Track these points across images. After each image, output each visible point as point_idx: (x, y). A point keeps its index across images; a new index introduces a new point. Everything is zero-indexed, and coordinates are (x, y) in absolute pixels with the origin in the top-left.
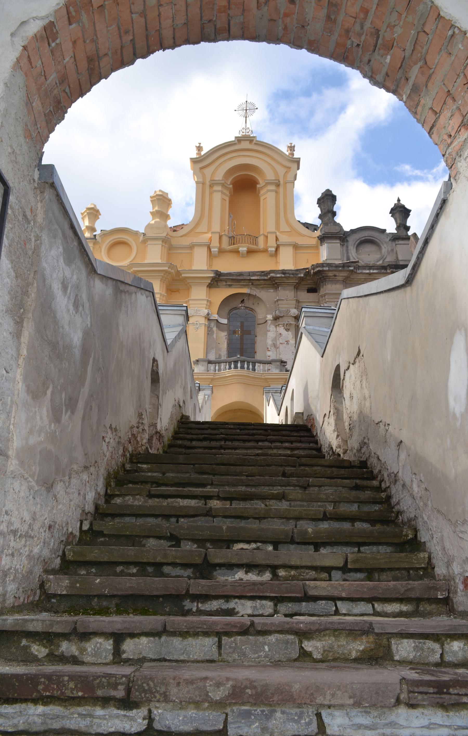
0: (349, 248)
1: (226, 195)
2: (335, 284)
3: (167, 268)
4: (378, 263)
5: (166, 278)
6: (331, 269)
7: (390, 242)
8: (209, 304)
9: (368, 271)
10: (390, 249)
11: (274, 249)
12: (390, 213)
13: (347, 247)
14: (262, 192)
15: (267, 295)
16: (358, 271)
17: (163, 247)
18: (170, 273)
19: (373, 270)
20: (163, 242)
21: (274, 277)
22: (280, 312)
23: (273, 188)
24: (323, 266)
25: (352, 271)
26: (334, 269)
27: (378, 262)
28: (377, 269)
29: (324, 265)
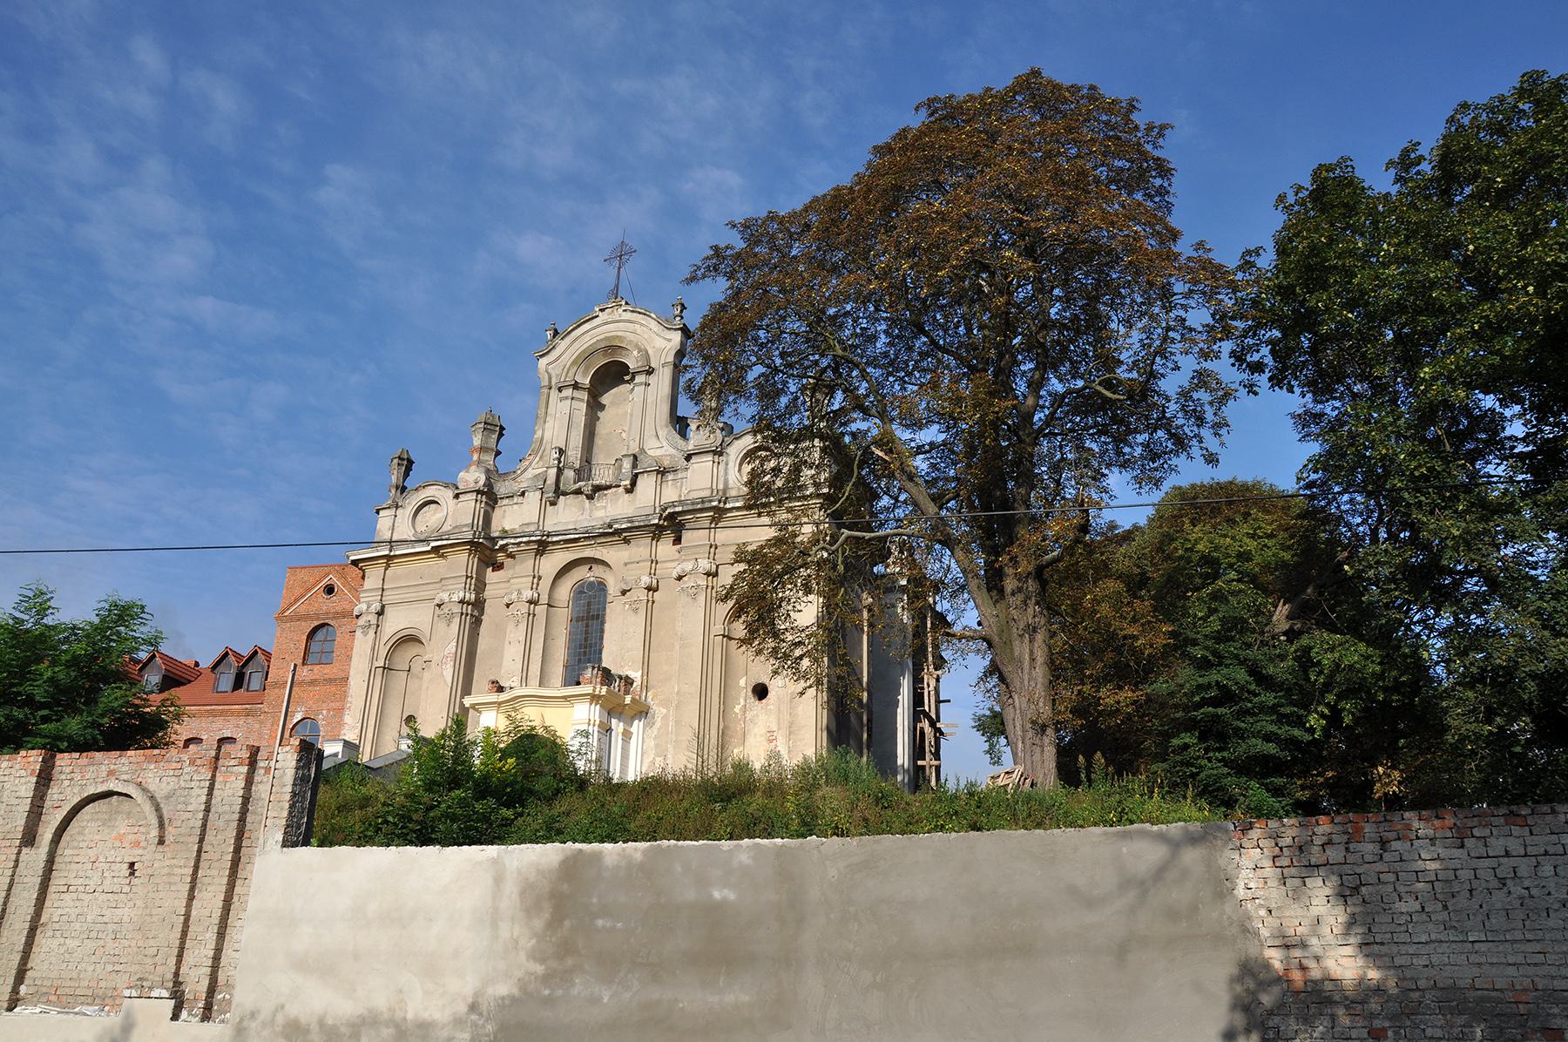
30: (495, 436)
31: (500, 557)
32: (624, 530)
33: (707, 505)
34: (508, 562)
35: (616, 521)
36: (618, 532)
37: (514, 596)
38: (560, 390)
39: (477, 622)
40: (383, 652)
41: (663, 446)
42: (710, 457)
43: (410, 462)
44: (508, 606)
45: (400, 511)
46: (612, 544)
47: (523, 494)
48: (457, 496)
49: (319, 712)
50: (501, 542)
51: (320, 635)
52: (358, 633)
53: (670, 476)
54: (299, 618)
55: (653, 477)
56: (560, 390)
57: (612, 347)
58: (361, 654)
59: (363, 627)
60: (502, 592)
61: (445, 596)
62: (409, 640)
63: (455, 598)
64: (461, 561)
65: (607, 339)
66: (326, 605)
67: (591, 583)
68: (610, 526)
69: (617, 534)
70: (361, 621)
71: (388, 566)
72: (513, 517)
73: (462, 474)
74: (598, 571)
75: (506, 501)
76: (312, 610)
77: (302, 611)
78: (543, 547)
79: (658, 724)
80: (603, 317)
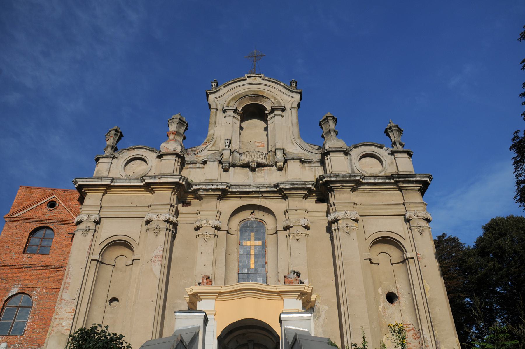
0: (353, 162)
1: (237, 119)
2: (343, 194)
3: (177, 180)
4: (381, 175)
5: (177, 191)
6: (338, 179)
7: (390, 156)
8: (218, 214)
9: (373, 181)
10: (390, 162)
11: (282, 164)
12: (385, 133)
13: (351, 160)
14: (269, 117)
15: (277, 205)
16: (364, 181)
17: (177, 162)
18: (181, 185)
19: (378, 179)
20: (176, 157)
21: (283, 188)
22: (290, 222)
23: (279, 112)
24: (331, 177)
25: (359, 180)
26: (342, 179)
27: (381, 172)
28: (382, 179)
29: (332, 175)
30: (184, 128)
31: (190, 198)
32: (286, 189)
33: (353, 178)
34: (194, 202)
35: (282, 183)
36: (281, 191)
37: (203, 223)
38: (224, 111)
39: (174, 237)
40: (98, 249)
41: (296, 148)
42: (342, 154)
43: (121, 135)
44: (197, 229)
45: (115, 161)
46: (273, 198)
47: (204, 162)
48: (160, 157)
49: (33, 289)
50: (195, 187)
51: (42, 233)
52: (79, 235)
53: (307, 165)
54: (25, 220)
55: (298, 163)
56: (224, 111)
57: (257, 96)
58: (80, 251)
59: (83, 230)
60: (192, 220)
61: (154, 217)
62: (122, 243)
63: (162, 218)
64: (167, 196)
65: (254, 91)
66: (48, 214)
67: (253, 222)
68: (276, 186)
69: (281, 192)
70: (81, 226)
71: (105, 193)
72: (195, 175)
73: (163, 145)
74: (259, 214)
75: (190, 166)
76: (36, 216)
77: (28, 215)
78: (224, 194)
79: (323, 317)
80: (249, 81)
